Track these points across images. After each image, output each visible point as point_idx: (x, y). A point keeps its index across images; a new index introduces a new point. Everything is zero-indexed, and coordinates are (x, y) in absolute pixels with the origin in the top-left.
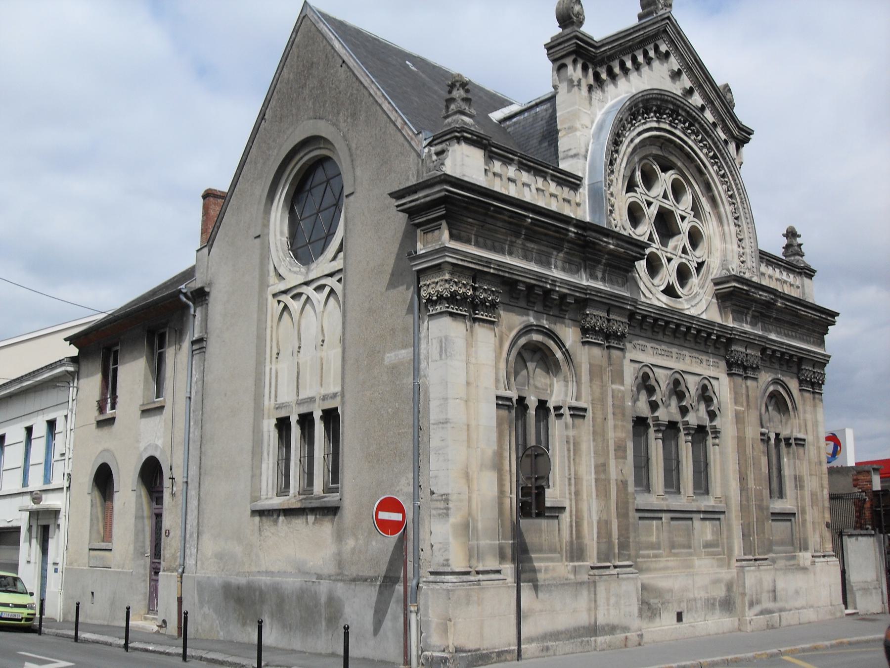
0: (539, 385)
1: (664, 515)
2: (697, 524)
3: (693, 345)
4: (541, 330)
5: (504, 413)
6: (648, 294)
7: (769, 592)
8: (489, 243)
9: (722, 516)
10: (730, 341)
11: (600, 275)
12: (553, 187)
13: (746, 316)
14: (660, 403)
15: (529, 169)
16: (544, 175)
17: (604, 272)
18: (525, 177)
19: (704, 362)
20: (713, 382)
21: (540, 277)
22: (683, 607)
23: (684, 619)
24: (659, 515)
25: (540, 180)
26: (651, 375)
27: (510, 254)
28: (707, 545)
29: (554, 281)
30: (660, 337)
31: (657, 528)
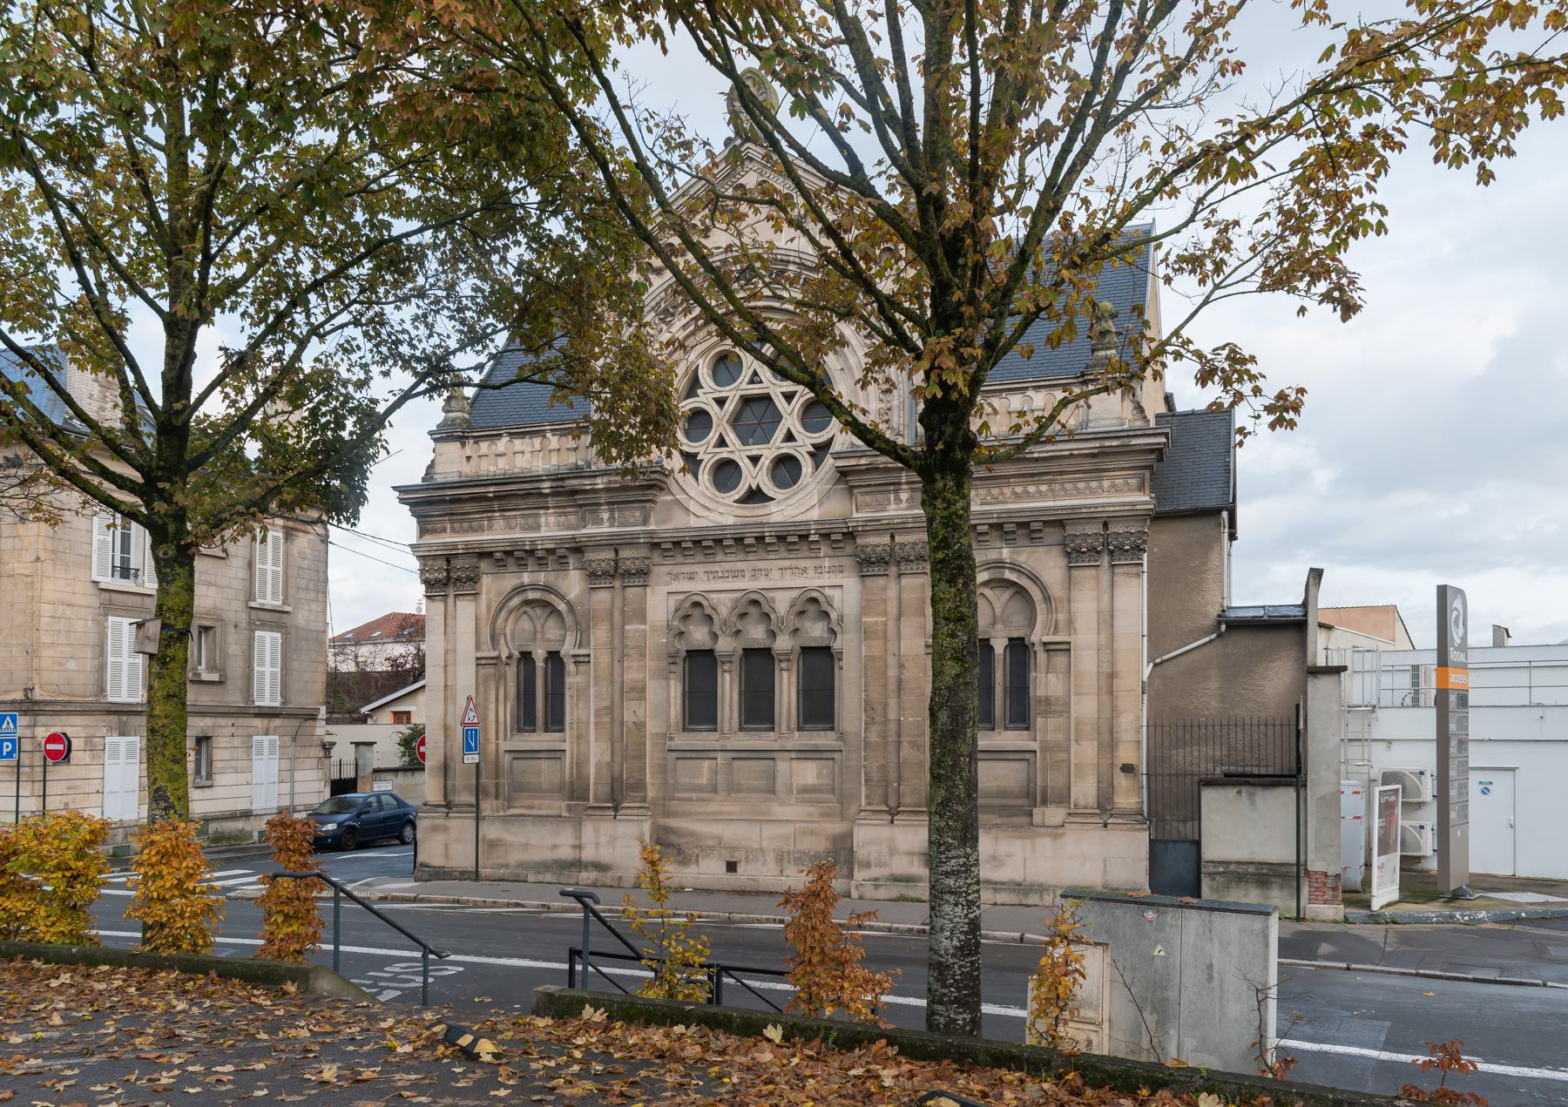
0: (549, 636)
1: (719, 755)
2: (782, 766)
3: (786, 555)
4: (534, 587)
5: (490, 670)
6: (700, 512)
7: (910, 854)
8: (465, 525)
9: (837, 756)
10: (850, 535)
11: (606, 516)
12: (554, 441)
13: (896, 491)
14: (719, 633)
15: (523, 435)
16: (542, 434)
17: (612, 511)
18: (518, 444)
19: (811, 572)
20: (827, 592)
21: (515, 542)
22: (738, 856)
23: (739, 870)
24: (712, 755)
25: (537, 441)
26: (705, 603)
27: (490, 528)
28: (805, 790)
29: (533, 542)
30: (720, 557)
31: (710, 769)
